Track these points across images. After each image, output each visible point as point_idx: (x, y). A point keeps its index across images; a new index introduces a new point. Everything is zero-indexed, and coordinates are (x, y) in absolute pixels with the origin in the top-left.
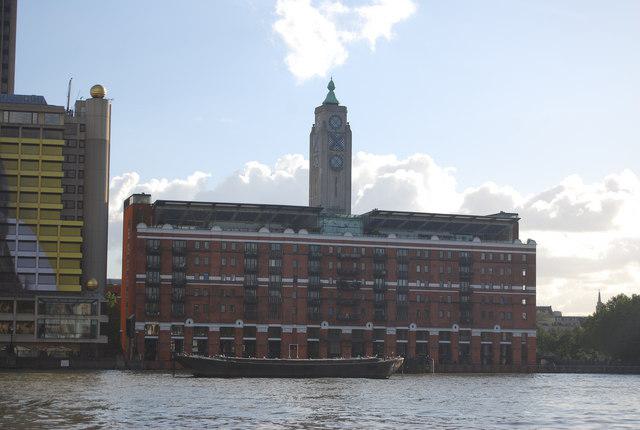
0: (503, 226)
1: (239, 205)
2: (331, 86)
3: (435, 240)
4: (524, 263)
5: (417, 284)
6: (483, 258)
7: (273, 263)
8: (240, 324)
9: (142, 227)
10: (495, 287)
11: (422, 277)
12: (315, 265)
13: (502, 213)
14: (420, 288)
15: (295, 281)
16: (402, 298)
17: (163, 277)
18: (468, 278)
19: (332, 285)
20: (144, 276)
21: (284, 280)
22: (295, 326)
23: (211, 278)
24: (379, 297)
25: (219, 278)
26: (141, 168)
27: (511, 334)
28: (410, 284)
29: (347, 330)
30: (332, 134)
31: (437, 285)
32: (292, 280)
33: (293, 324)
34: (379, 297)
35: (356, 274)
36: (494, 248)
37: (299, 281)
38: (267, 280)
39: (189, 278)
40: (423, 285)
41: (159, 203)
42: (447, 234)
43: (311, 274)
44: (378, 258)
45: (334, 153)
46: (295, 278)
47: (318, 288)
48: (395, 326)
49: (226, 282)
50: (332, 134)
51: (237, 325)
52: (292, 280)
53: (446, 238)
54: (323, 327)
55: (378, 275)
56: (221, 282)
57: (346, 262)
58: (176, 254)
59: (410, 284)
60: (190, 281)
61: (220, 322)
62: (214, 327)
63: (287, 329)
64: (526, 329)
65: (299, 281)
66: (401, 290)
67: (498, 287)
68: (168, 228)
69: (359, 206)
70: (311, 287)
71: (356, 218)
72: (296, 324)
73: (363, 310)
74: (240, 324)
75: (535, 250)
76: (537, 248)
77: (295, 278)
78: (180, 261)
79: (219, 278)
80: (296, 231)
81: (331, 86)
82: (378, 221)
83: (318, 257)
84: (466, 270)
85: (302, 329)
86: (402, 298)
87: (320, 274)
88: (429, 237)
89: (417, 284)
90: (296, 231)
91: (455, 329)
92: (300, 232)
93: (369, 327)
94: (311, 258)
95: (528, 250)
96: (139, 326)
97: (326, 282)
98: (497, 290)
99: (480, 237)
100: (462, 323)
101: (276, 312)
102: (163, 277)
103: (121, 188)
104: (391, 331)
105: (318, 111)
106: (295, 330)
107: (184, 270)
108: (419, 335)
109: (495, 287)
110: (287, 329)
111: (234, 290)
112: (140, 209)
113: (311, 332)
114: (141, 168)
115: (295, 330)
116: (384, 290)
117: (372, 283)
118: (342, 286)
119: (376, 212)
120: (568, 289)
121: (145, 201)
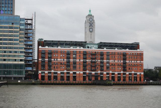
0: (135, 46)
2: (90, 11)
3: (116, 49)
4: (141, 56)
5: (112, 61)
6: (129, 54)
7: (74, 56)
8: (65, 71)
9: (40, 47)
10: (132, 61)
11: (112, 59)
13: (135, 43)
14: (112, 62)
17: (46, 59)
18: (125, 59)
19: (89, 61)
20: (41, 59)
21: (77, 60)
22: (80, 72)
24: (102, 64)
25: (60, 60)
26: (41, 33)
27: (137, 73)
28: (110, 61)
29: (93, 73)
30: (90, 22)
31: (117, 61)
32: (79, 60)
34: (102, 64)
35: (94, 59)
36: (111, 51)
38: (72, 60)
39: (52, 60)
40: (113, 61)
41: (45, 41)
42: (121, 48)
43: (84, 59)
44: (102, 54)
45: (91, 28)
46: (80, 60)
48: (106, 72)
49: (62, 61)
50: (90, 22)
51: (65, 72)
54: (87, 72)
56: (61, 61)
57: (94, 55)
58: (49, 54)
59: (110, 61)
60: (53, 60)
65: (81, 60)
66: (108, 63)
67: (133, 62)
68: (47, 47)
69: (97, 41)
73: (98, 68)
74: (65, 71)
77: (80, 60)
79: (60, 60)
80: (80, 48)
81: (90, 11)
82: (101, 45)
83: (85, 54)
88: (115, 49)
89: (112, 61)
90: (80, 48)
92: (81, 48)
93: (99, 72)
95: (141, 52)
96: (40, 72)
97: (88, 60)
98: (133, 62)
99: (128, 49)
101: (75, 68)
103: (37, 37)
105: (87, 17)
109: (132, 61)
110: (78, 72)
112: (42, 43)
113: (84, 73)
114: (41, 33)
117: (100, 61)
118: (92, 62)
119: (101, 43)
120: (150, 62)
121: (42, 41)
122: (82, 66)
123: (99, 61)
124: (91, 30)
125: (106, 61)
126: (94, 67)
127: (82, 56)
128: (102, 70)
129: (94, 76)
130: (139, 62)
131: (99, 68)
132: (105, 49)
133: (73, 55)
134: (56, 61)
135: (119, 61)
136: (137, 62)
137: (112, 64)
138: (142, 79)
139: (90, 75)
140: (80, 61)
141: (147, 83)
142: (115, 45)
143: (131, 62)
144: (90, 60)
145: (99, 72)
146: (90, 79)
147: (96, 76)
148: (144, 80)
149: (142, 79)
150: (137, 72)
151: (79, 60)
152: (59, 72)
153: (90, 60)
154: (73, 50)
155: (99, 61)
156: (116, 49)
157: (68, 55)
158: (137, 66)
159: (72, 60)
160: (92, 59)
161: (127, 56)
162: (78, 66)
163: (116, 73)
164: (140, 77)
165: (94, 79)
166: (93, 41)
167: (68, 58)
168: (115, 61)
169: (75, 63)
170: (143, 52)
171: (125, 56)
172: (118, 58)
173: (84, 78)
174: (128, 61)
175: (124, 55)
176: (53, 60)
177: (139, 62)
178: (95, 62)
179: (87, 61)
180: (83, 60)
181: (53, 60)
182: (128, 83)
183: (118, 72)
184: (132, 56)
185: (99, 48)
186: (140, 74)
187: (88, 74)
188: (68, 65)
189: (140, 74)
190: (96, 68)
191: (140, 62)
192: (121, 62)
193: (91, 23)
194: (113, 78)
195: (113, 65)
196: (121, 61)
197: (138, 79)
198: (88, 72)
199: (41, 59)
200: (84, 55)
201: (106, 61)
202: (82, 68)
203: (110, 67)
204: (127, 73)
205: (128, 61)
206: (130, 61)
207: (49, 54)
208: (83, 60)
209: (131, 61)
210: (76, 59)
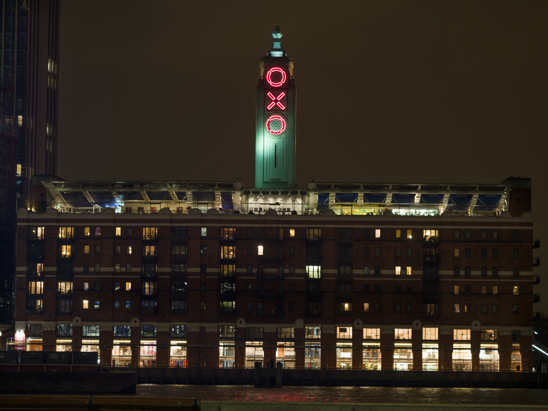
5: (366, 270)
6: (457, 236)
10: (473, 273)
14: (369, 275)
15: (203, 272)
21: (190, 270)
22: (203, 324)
23: (103, 269)
28: (355, 272)
33: (201, 321)
37: (209, 270)
38: (168, 270)
39: (76, 269)
40: (372, 272)
52: (198, 270)
59: (355, 272)
65: (209, 270)
67: (478, 273)
77: (203, 267)
79: (111, 269)
89: (366, 270)
98: (476, 277)
106: (202, 329)
109: (473, 273)
115: (202, 329)
134: (91, 273)
144: (255, 271)
151: (198, 270)
159: (168, 270)
170: (530, 224)
174: (451, 273)
176: (81, 269)
177: (510, 273)
181: (81, 269)
199: (24, 269)
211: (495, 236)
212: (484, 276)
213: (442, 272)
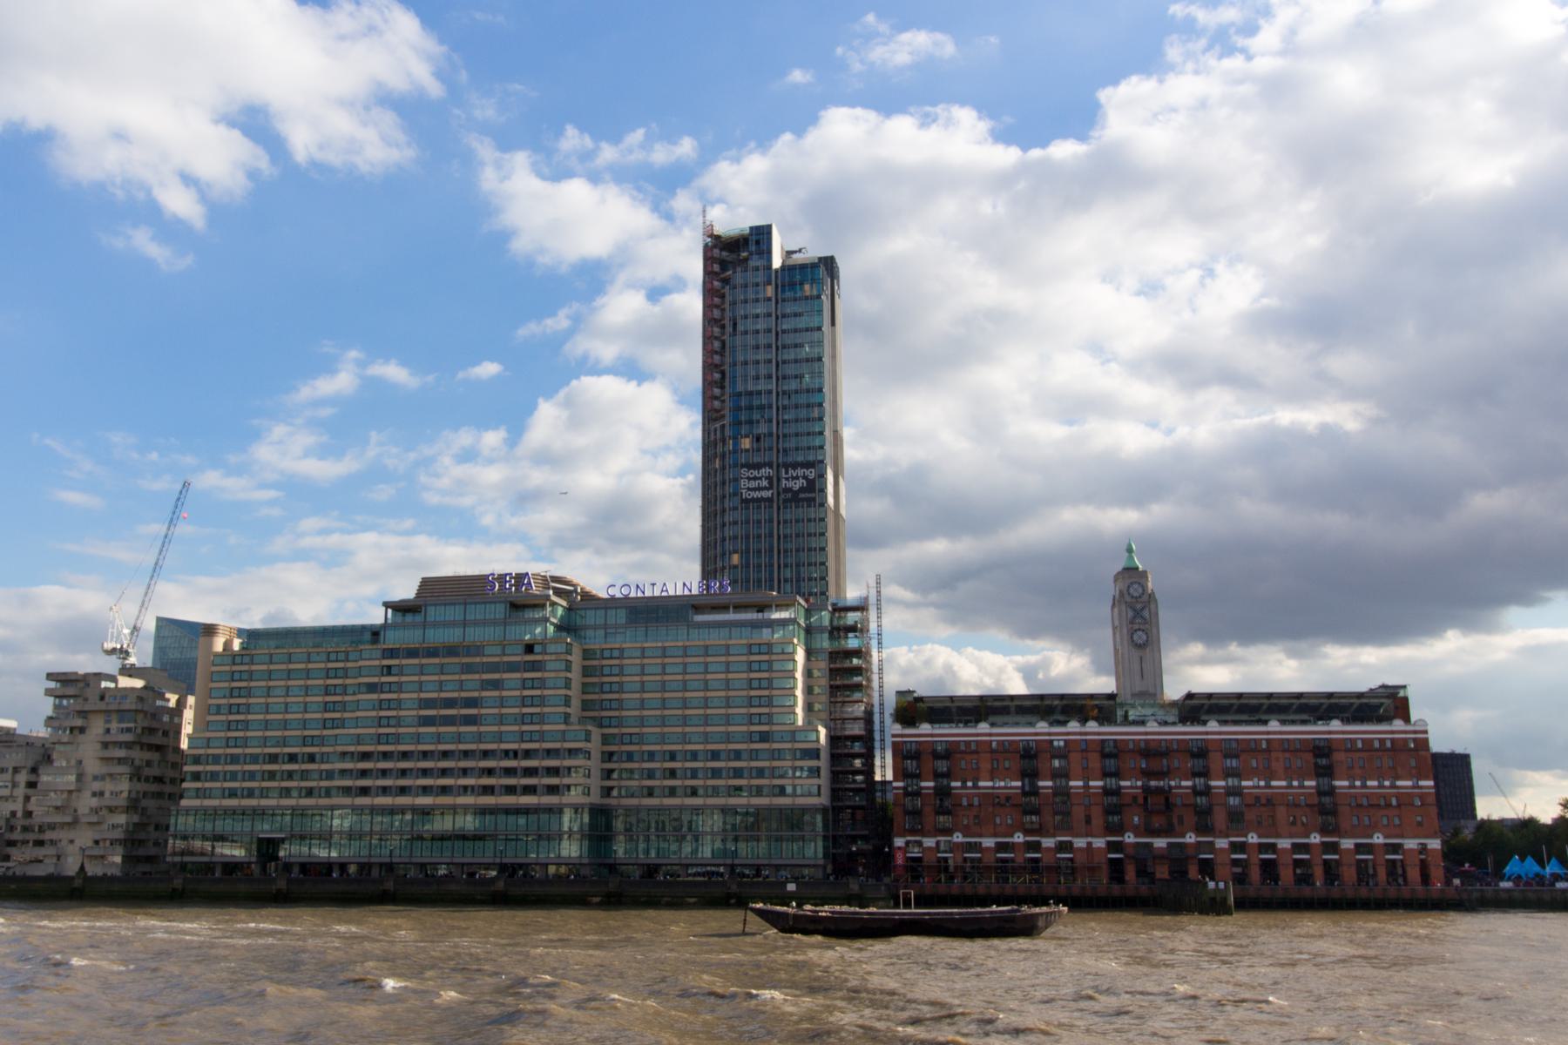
1: (1270, 696)
7: (1056, 763)
10: (1369, 783)
12: (1111, 764)
15: (1086, 787)
16: (1233, 801)
17: (923, 784)
18: (1326, 772)
21: (1072, 783)
25: (990, 784)
28: (1244, 783)
29: (1160, 843)
31: (1284, 783)
38: (1050, 783)
39: (954, 784)
40: (1262, 783)
42: (1305, 717)
43: (1105, 775)
44: (1200, 751)
46: (1086, 779)
47: (1117, 792)
48: (1227, 836)
52: (1080, 783)
53: (1225, 722)
55: (1195, 775)
59: (1244, 783)
61: (995, 835)
62: (988, 842)
63: (1080, 843)
64: (1427, 837)
67: (1375, 783)
68: (925, 728)
70: (1107, 792)
71: (1174, 704)
72: (1092, 836)
75: (1426, 732)
76: (1429, 728)
78: (942, 766)
79: (990, 784)
84: (1324, 762)
85: (1099, 843)
86: (1233, 801)
87: (1117, 775)
88: (1265, 722)
91: (1315, 839)
93: (1190, 838)
94: (1105, 756)
96: (899, 842)
97: (1127, 783)
100: (1324, 831)
102: (923, 784)
104: (1222, 843)
105: (1117, 577)
106: (1089, 844)
107: (948, 775)
108: (1263, 848)
109: (1369, 783)
110: (1080, 843)
111: (1008, 798)
112: (912, 709)
113: (1112, 847)
115: (1089, 844)
116: (1207, 791)
117: (1189, 783)
118: (1147, 790)
119: (1190, 696)
122: (1096, 813)
123: (1184, 783)
124: (1140, 637)
125: (1222, 783)
126: (1160, 810)
127: (1095, 762)
128: (1204, 828)
129: (1163, 857)
130: (1409, 783)
131: (1191, 819)
132: (1213, 726)
133: (1054, 757)
135: (1295, 783)
136: (1399, 783)
137: (1257, 798)
138: (1437, 873)
139: (1144, 860)
140: (1086, 787)
141: (1530, 895)
142: (1331, 705)
143: (1364, 786)
144: (1139, 783)
145: (1190, 838)
146: (1142, 872)
147: (1178, 859)
148: (1448, 883)
149: (1437, 873)
150: (1402, 836)
151: (1080, 783)
152: (988, 842)
153: (1139, 783)
154: (1049, 734)
155: (1184, 783)
156: (1274, 725)
157: (1029, 759)
158: (1399, 805)
159: (1050, 783)
160: (1148, 774)
161: (1338, 757)
162: (1078, 812)
163: (1284, 843)
164: (1422, 861)
165: (1166, 876)
166: (1151, 690)
167: (1030, 775)
168: (1274, 783)
169: (1063, 793)
171: (1328, 756)
172: (1286, 769)
173: (1116, 868)
174: (1346, 783)
175: (1322, 757)
176: (958, 784)
178: (1159, 790)
179: (1120, 787)
180: (1100, 783)
182: (1350, 893)
183: (1291, 836)
184: (1365, 755)
185: (1183, 720)
186: (1423, 849)
187: (1130, 851)
188: (1027, 807)
189: (1423, 849)
190: (1175, 821)
191: (1413, 787)
192: (1303, 787)
193: (1139, 606)
194: (1269, 868)
195: (1270, 802)
196: (1307, 783)
197: (1414, 874)
198: (1130, 838)
200: (1105, 756)
201: (1222, 783)
202: (1098, 821)
203: (1250, 815)
204: (1347, 844)
205: (1346, 783)
206: (1358, 783)
207: (936, 756)
208: (1100, 783)
209: (1364, 779)
210: (1067, 777)
211: (1389, 744)
212: (1381, 786)
213: (1337, 783)
